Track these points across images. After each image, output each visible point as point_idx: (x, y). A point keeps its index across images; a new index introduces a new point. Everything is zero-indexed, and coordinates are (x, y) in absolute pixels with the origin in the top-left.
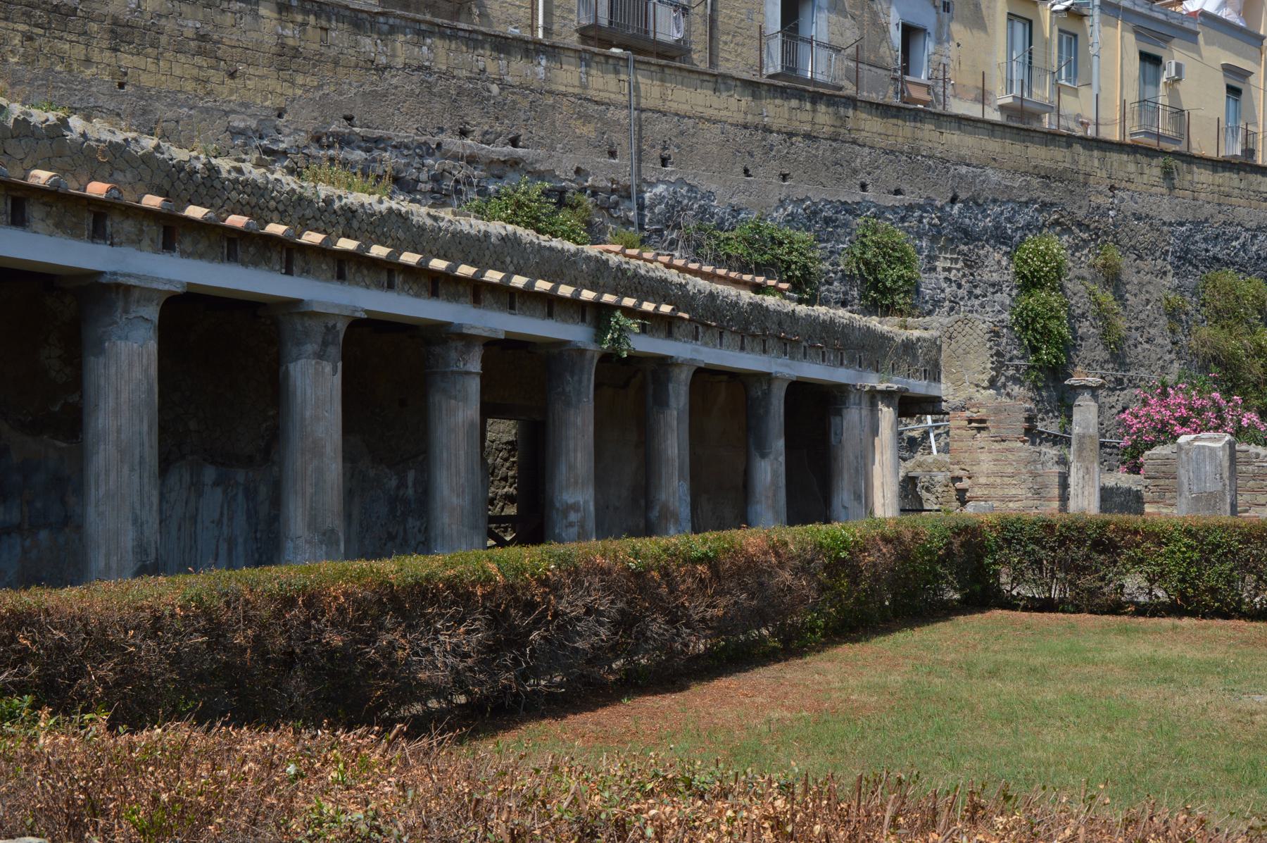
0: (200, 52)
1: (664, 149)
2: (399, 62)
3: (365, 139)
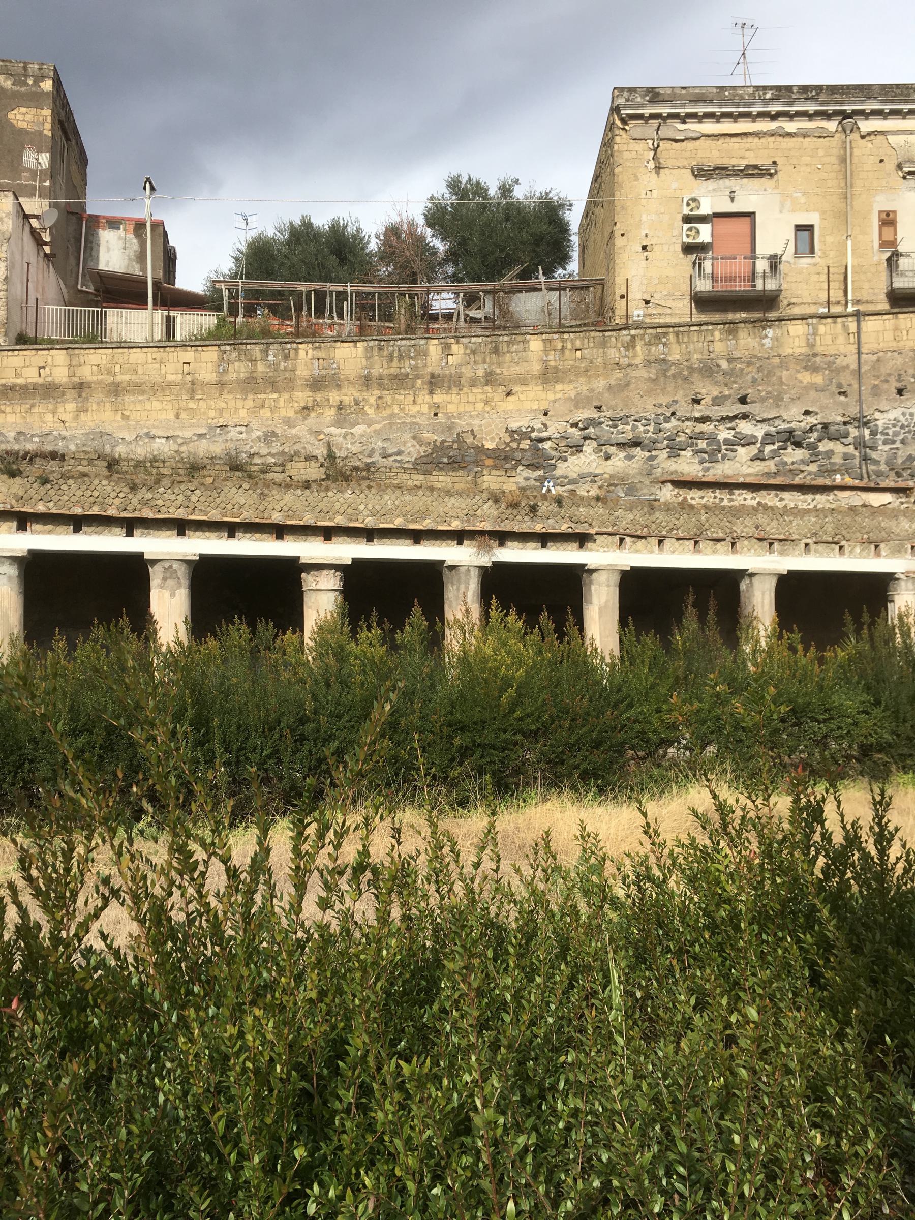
0: (488, 383)
2: (638, 361)
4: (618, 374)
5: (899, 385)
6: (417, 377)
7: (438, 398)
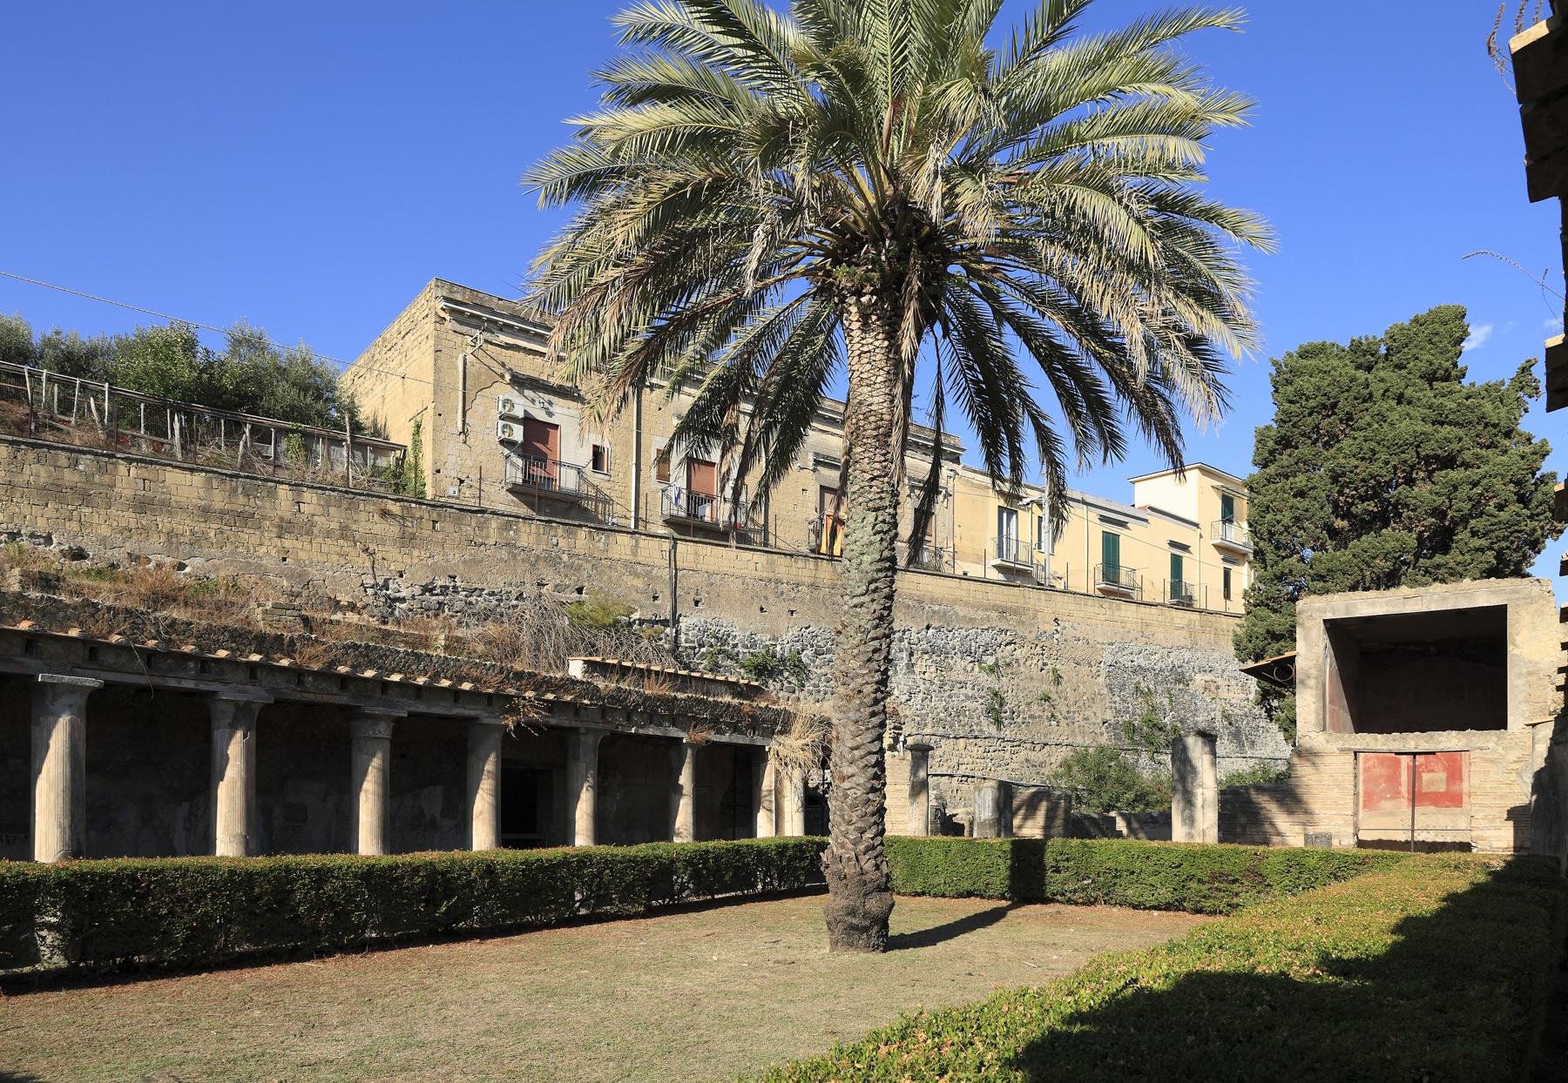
1: (697, 594)
4: (472, 550)
5: (697, 598)
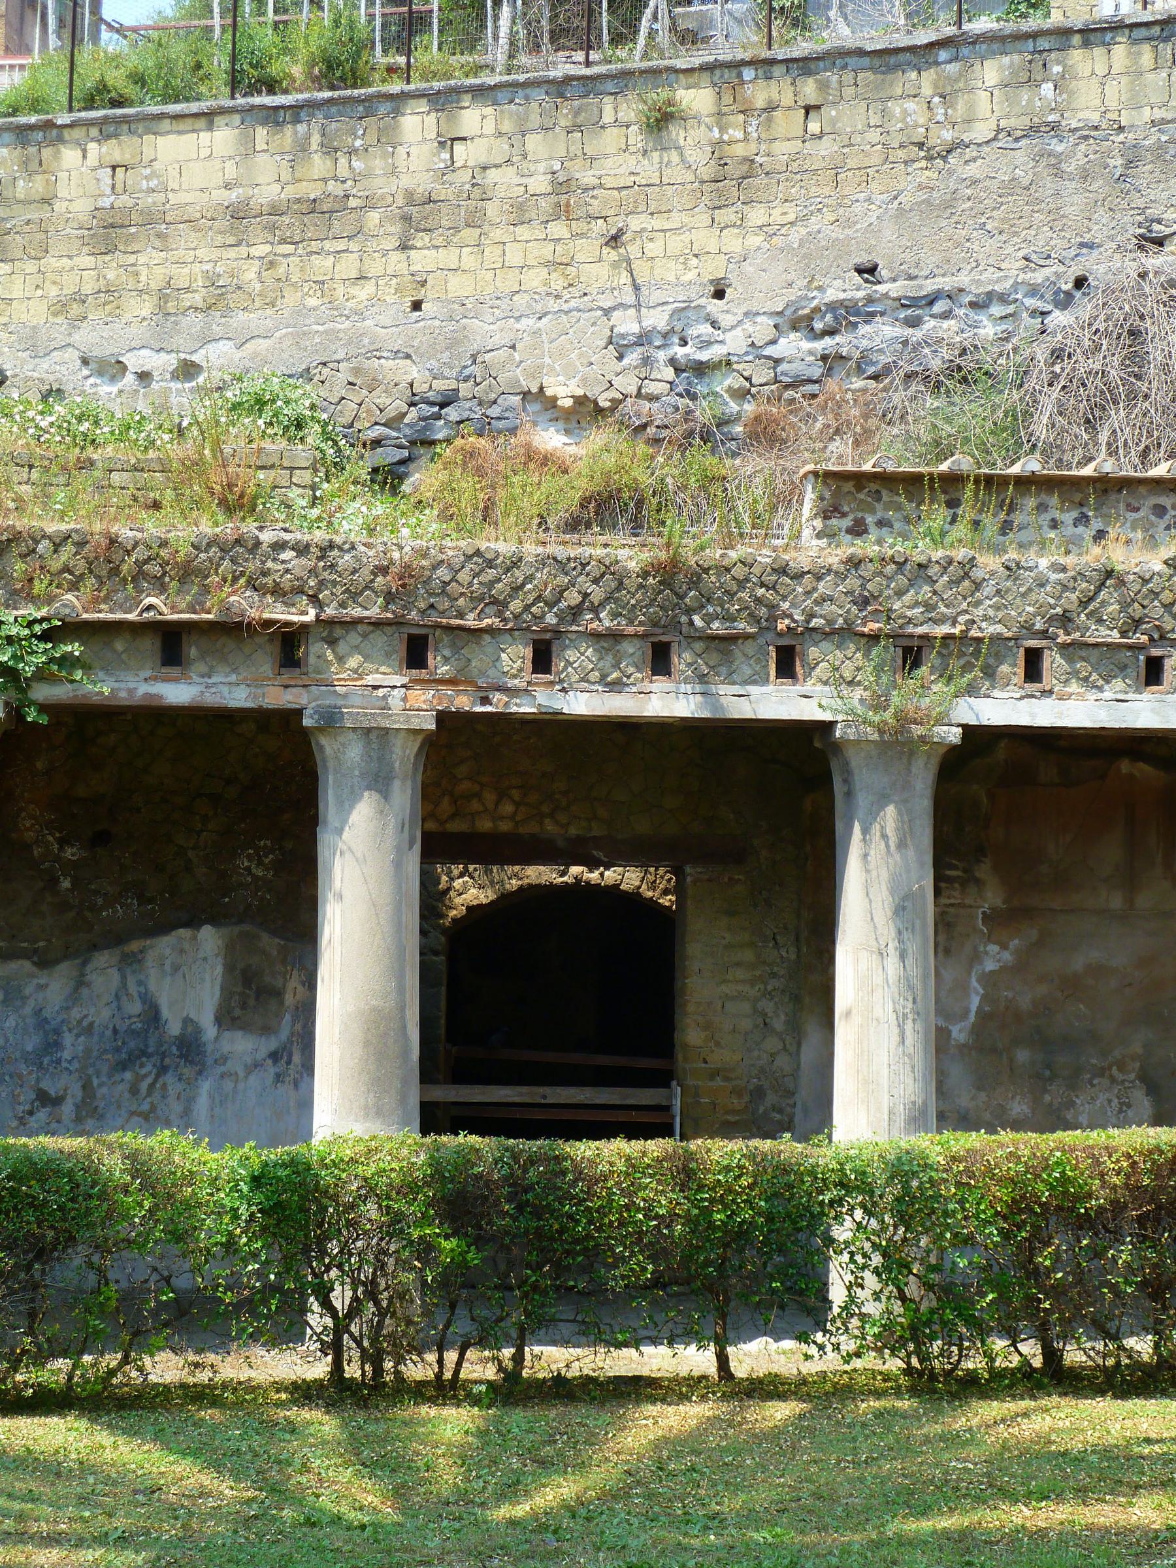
3: (903, 303)
6: (369, 203)
7: (422, 260)
